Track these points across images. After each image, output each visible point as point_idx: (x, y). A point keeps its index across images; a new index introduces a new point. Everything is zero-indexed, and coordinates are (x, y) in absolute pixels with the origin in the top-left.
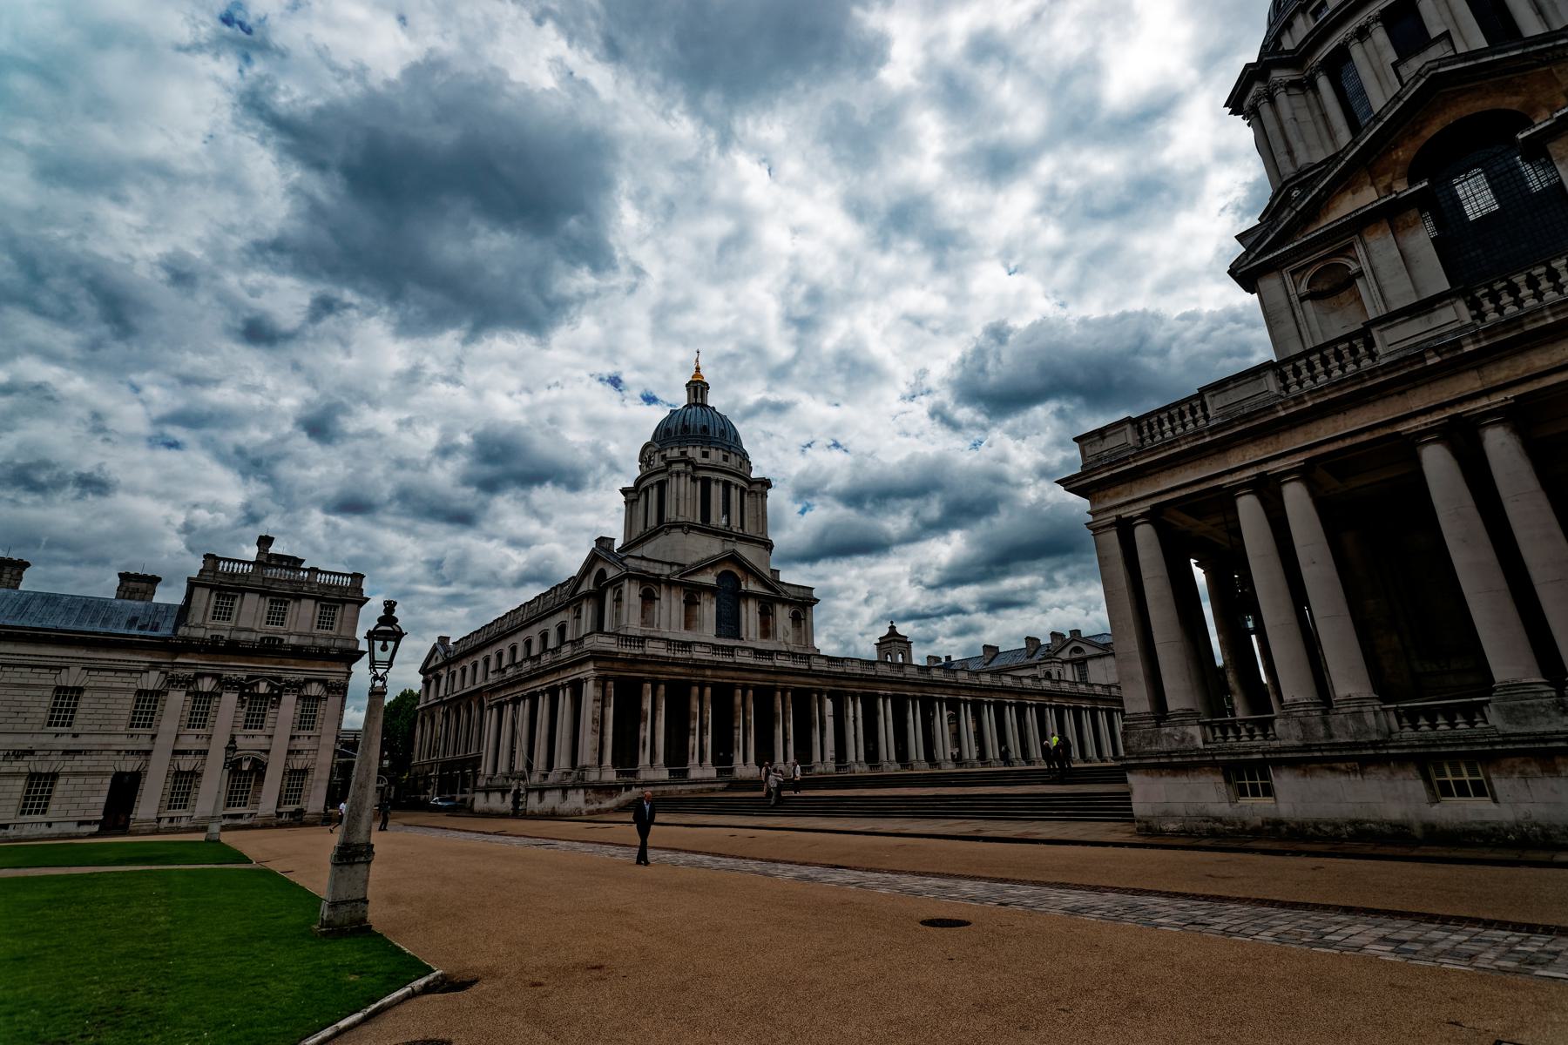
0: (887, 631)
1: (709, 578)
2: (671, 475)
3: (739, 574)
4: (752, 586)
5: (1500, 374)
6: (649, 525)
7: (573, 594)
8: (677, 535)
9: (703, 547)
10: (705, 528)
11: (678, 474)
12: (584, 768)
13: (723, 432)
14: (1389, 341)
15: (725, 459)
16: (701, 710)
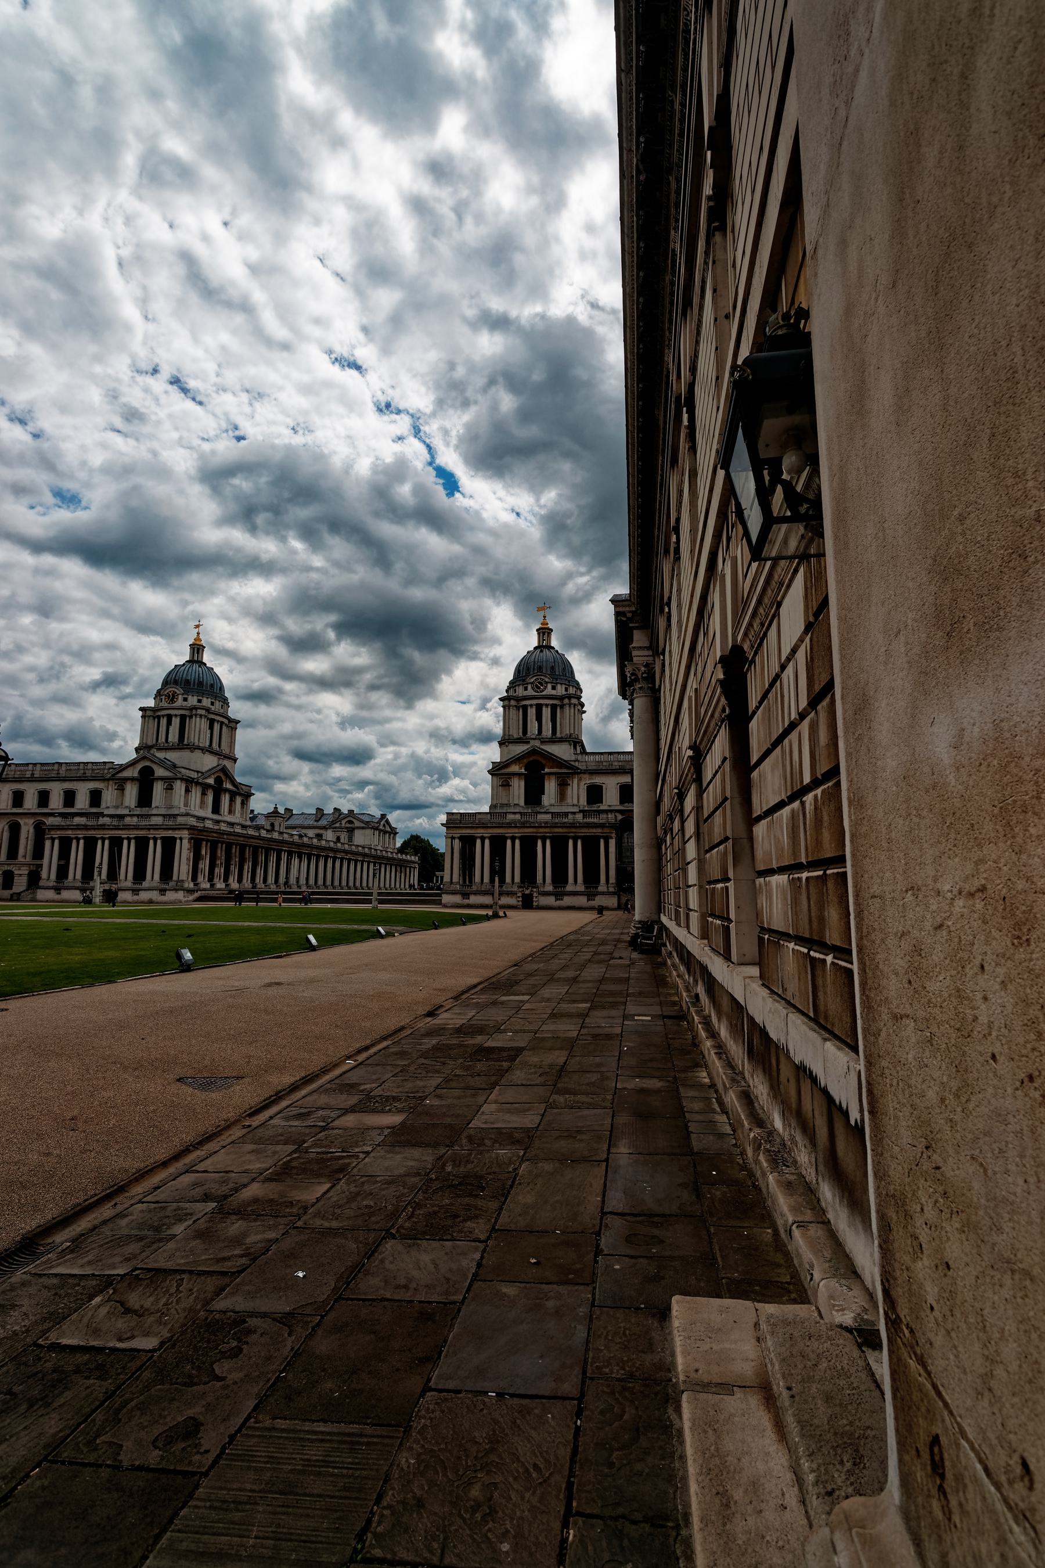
0: (272, 810)
1: (211, 781)
2: (196, 715)
3: (223, 778)
4: (229, 786)
5: (521, 830)
6: (170, 740)
7: (113, 775)
8: (198, 754)
9: (209, 762)
10: (209, 750)
11: (201, 716)
12: (183, 881)
13: (212, 686)
14: (510, 817)
15: (212, 704)
16: (221, 853)
